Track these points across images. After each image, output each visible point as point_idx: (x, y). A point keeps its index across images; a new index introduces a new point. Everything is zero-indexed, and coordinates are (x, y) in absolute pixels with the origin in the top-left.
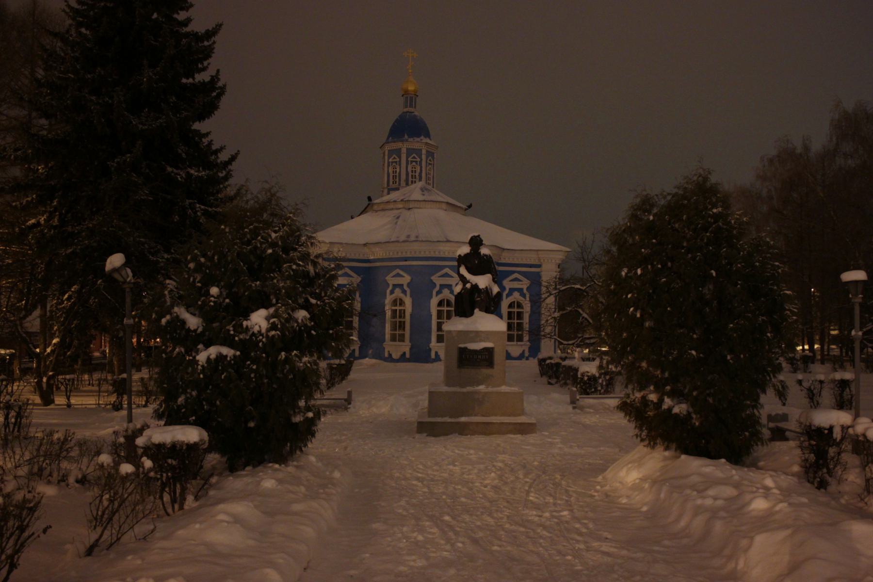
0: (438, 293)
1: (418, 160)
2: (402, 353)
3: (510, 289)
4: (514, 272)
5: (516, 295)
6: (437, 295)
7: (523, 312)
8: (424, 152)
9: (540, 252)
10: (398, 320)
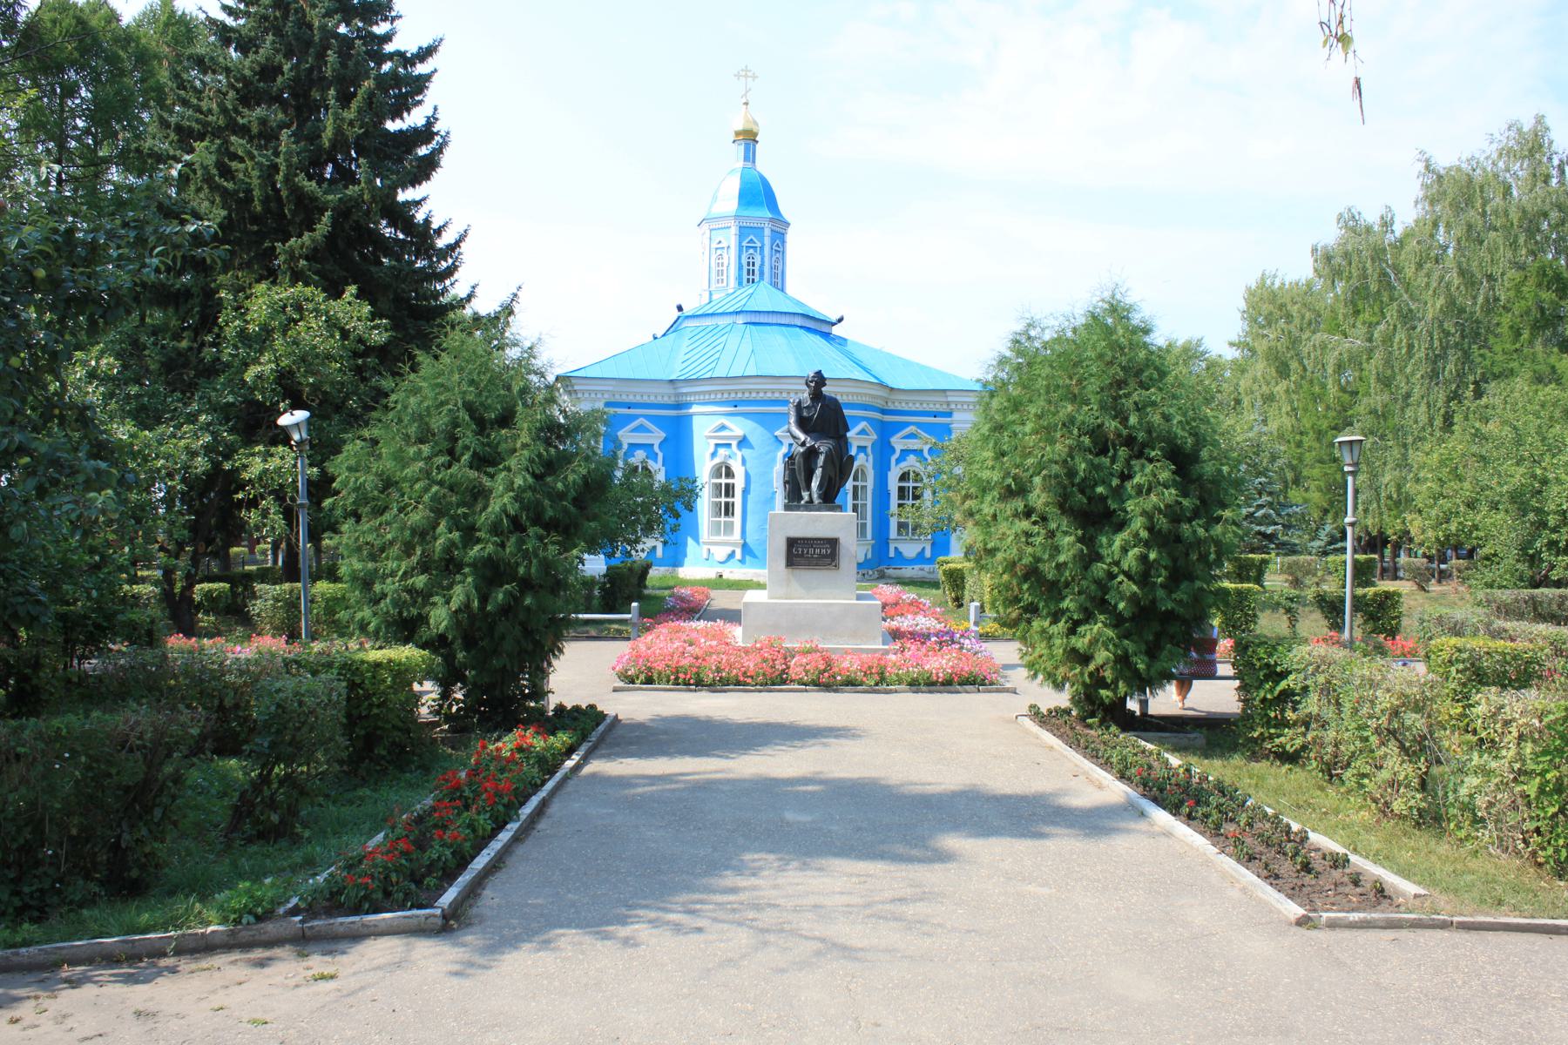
1: (759, 245)
4: (908, 424)
5: (912, 458)
8: (767, 232)
10: (723, 499)
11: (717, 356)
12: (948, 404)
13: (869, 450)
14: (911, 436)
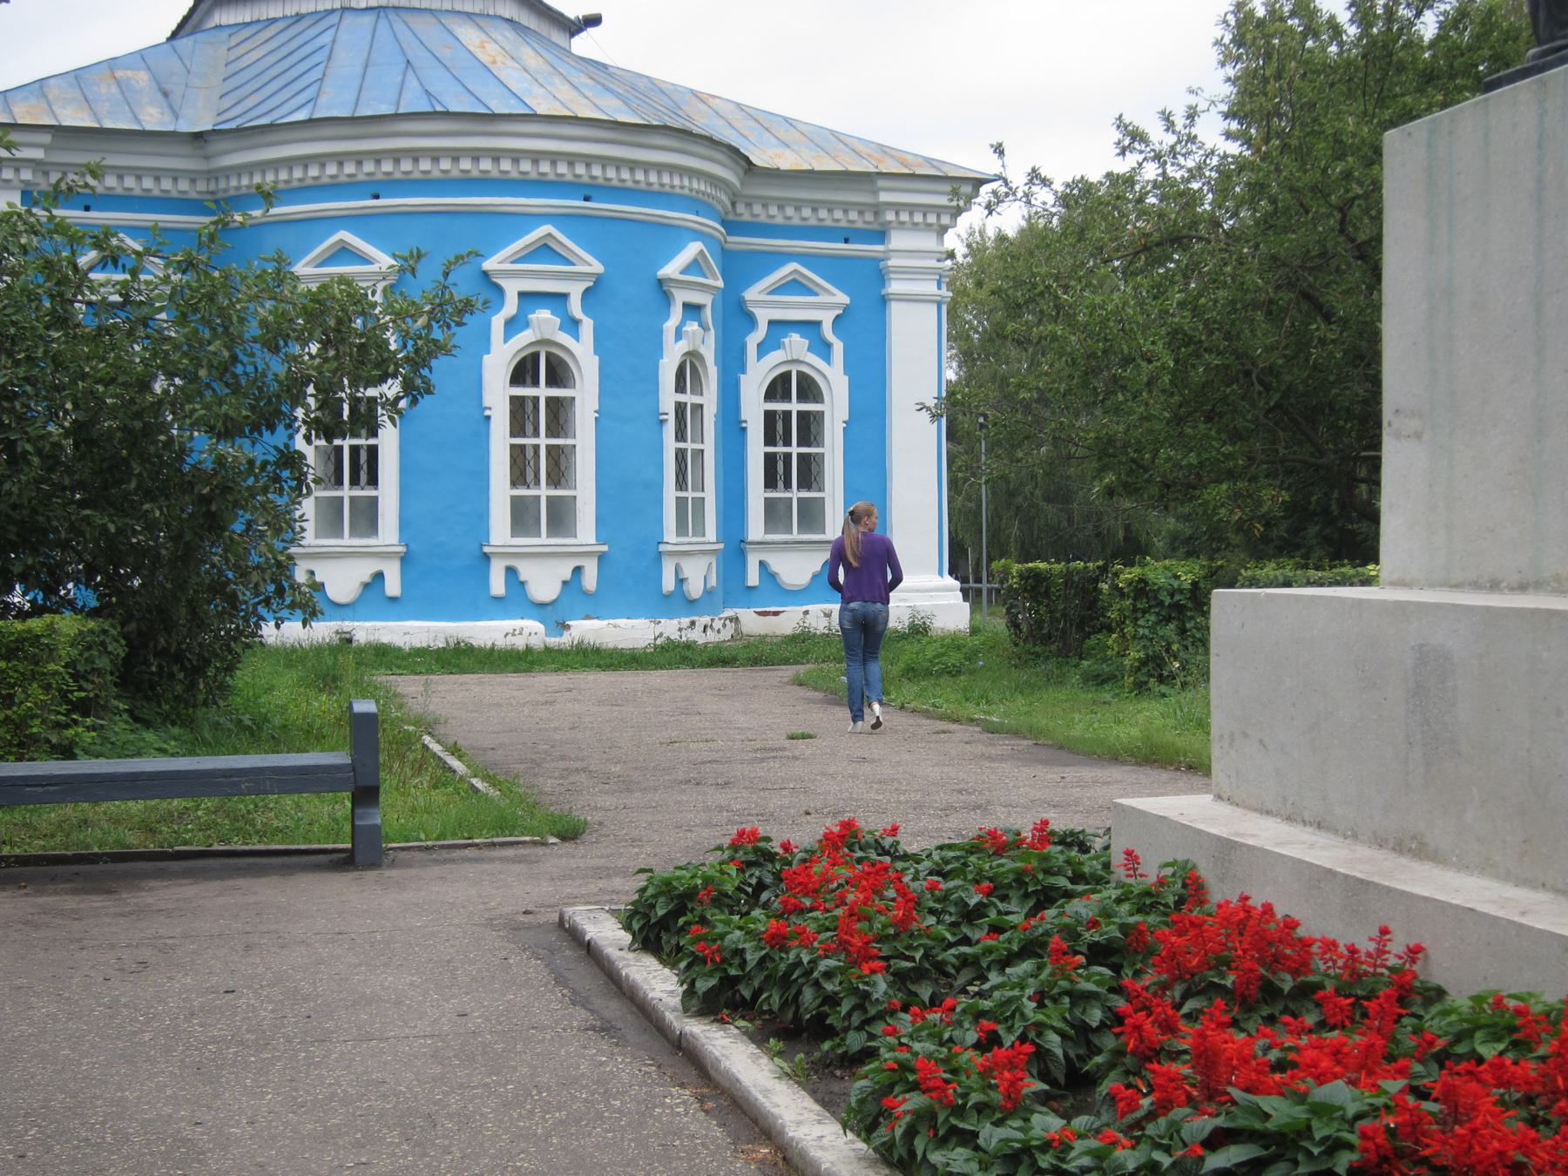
0: (513, 326)
2: (367, 579)
3: (771, 323)
5: (796, 343)
6: (507, 337)
7: (822, 413)
9: (881, 183)
11: (315, 74)
12: (878, 209)
13: (708, 312)
14: (795, 286)
